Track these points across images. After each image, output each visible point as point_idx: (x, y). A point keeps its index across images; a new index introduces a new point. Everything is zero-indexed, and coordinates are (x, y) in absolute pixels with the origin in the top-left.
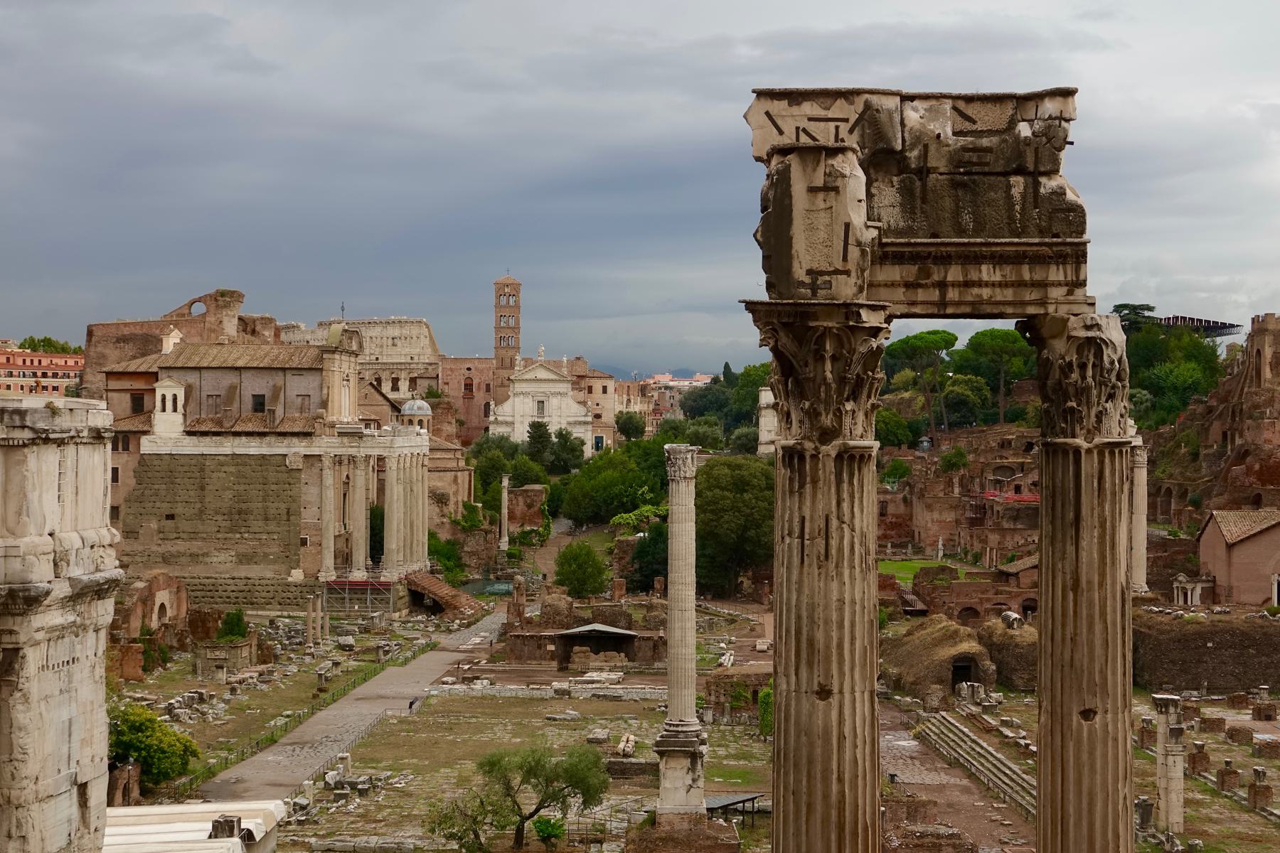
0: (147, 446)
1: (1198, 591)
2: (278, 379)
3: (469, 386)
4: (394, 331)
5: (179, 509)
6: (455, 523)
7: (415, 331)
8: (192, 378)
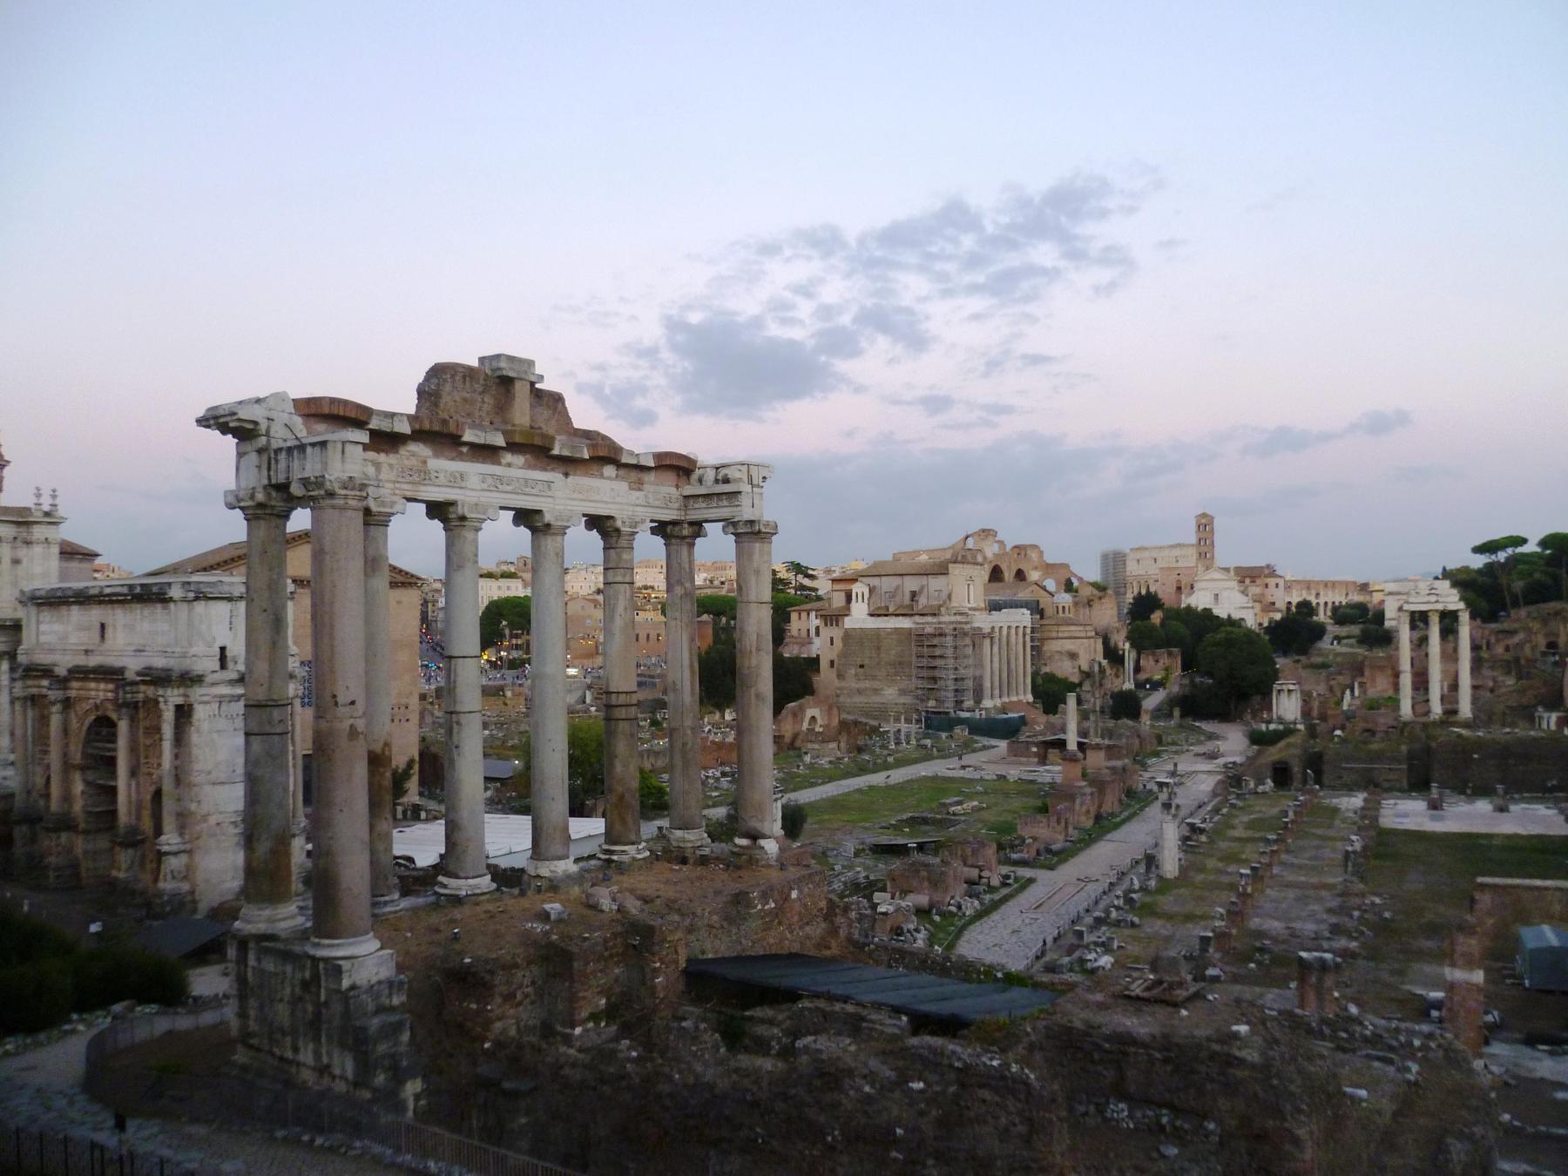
0: (848, 623)
2: (924, 580)
3: (1179, 588)
4: (1177, 552)
5: (866, 662)
6: (1081, 671)
8: (875, 582)
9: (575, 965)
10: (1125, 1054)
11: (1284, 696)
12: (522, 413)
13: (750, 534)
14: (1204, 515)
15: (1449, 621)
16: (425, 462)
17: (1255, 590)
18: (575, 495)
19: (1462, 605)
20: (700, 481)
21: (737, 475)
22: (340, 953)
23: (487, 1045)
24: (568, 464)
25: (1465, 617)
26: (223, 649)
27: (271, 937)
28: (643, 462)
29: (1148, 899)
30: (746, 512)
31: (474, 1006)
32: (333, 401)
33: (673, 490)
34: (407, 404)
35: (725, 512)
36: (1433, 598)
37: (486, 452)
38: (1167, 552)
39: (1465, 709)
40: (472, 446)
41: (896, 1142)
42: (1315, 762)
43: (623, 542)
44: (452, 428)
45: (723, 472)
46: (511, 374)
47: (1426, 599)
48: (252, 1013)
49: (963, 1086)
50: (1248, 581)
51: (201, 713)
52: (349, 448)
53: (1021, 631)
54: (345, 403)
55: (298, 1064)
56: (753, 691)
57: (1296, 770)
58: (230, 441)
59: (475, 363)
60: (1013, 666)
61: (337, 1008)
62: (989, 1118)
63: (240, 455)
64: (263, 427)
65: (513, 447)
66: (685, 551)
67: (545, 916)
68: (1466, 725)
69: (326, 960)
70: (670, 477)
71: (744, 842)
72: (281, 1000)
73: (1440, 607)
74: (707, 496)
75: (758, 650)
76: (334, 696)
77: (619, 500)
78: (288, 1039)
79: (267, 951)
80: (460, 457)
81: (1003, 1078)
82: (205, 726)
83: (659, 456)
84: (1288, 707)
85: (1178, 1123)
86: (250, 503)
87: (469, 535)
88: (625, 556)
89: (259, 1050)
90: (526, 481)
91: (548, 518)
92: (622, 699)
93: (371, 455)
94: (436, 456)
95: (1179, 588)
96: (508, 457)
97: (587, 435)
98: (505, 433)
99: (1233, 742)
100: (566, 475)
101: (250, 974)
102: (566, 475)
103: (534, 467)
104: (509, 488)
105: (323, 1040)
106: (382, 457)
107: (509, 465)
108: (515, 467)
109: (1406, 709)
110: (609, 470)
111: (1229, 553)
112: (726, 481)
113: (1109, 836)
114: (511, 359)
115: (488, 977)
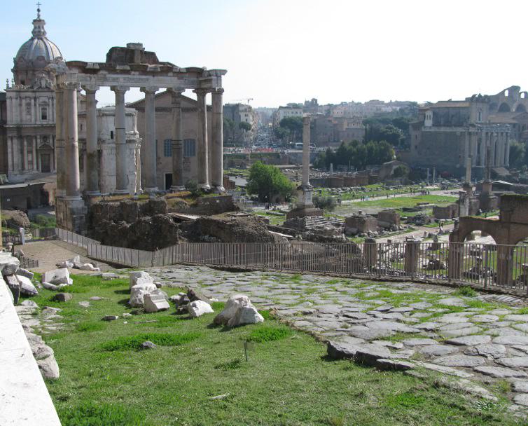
12: (138, 60)
26: (112, 132)
28: (181, 71)
33: (195, 79)
34: (103, 60)
51: (105, 152)
53: (504, 134)
59: (126, 46)
74: (205, 81)
80: (117, 73)
82: (106, 158)
90: (140, 79)
93: (88, 75)
96: (133, 73)
100: (154, 76)
102: (154, 76)
103: (142, 75)
106: (92, 75)
108: (135, 75)
110: (170, 74)
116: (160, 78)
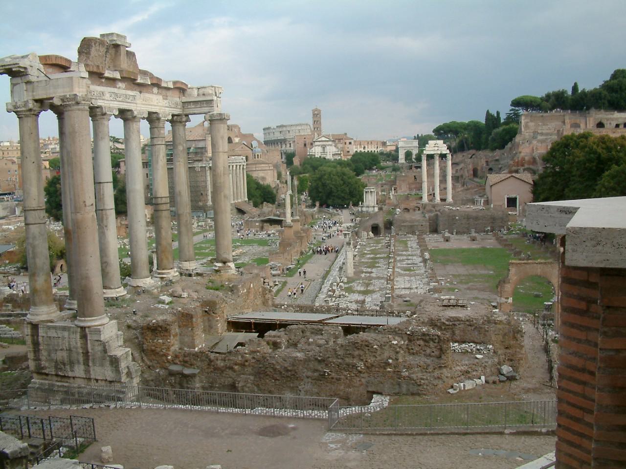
1: (482, 201)
3: (305, 145)
4: (299, 128)
7: (305, 127)
9: (194, 320)
10: (454, 325)
11: (369, 195)
12: (124, 63)
13: (216, 120)
14: (316, 110)
15: (443, 156)
16: (89, 87)
17: (340, 146)
18: (144, 102)
19: (448, 152)
20: (190, 95)
21: (210, 92)
22: (96, 323)
23: (169, 358)
24: (141, 86)
25: (449, 157)
27: (52, 322)
29: (347, 286)
30: (216, 111)
31: (161, 341)
32: (57, 57)
33: (178, 99)
35: (206, 109)
36: (436, 148)
37: (112, 81)
38: (293, 128)
39: (450, 199)
40: (108, 79)
41: (389, 364)
42: (389, 225)
43: (161, 125)
44: (101, 71)
45: (201, 91)
46: (120, 43)
47: (434, 148)
48: (43, 358)
49: (410, 341)
50: (337, 141)
52: (81, 80)
53: (242, 167)
54: (61, 58)
55: (74, 378)
56: (222, 194)
57: (381, 225)
58: (6, 78)
59: (99, 37)
60: (239, 185)
61: (100, 348)
62: (421, 351)
63: (13, 85)
64: (30, 71)
65: (123, 79)
66: (181, 128)
67: (163, 302)
68: (449, 205)
69: (89, 327)
70: (177, 93)
71: (220, 265)
72: (61, 350)
73: (439, 152)
75: (224, 174)
76: (85, 202)
77: (159, 104)
78: (68, 367)
79: (49, 328)
80: (101, 84)
81: (428, 335)
83: (175, 83)
84: (370, 200)
85: (478, 347)
86: (23, 109)
87: (106, 122)
88: (162, 132)
89: (47, 375)
90: (126, 95)
91: (135, 113)
92: (164, 200)
94: (92, 84)
95: (305, 145)
96: (120, 84)
97: (145, 73)
98: (121, 71)
99: (345, 217)
100: (141, 92)
101: (40, 339)
104: (120, 99)
105: (90, 364)
107: (119, 88)
109: (425, 199)
110: (155, 90)
111: (329, 127)
112: (204, 94)
113: (309, 261)
114: (118, 35)
115: (168, 327)
116: (147, 95)
